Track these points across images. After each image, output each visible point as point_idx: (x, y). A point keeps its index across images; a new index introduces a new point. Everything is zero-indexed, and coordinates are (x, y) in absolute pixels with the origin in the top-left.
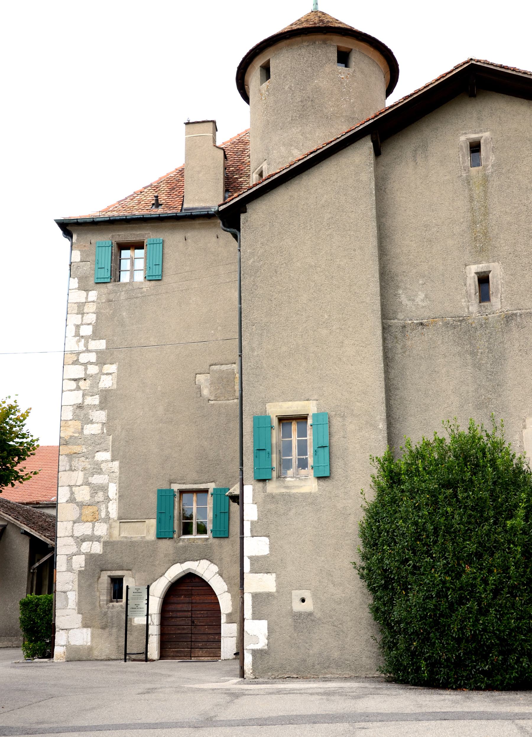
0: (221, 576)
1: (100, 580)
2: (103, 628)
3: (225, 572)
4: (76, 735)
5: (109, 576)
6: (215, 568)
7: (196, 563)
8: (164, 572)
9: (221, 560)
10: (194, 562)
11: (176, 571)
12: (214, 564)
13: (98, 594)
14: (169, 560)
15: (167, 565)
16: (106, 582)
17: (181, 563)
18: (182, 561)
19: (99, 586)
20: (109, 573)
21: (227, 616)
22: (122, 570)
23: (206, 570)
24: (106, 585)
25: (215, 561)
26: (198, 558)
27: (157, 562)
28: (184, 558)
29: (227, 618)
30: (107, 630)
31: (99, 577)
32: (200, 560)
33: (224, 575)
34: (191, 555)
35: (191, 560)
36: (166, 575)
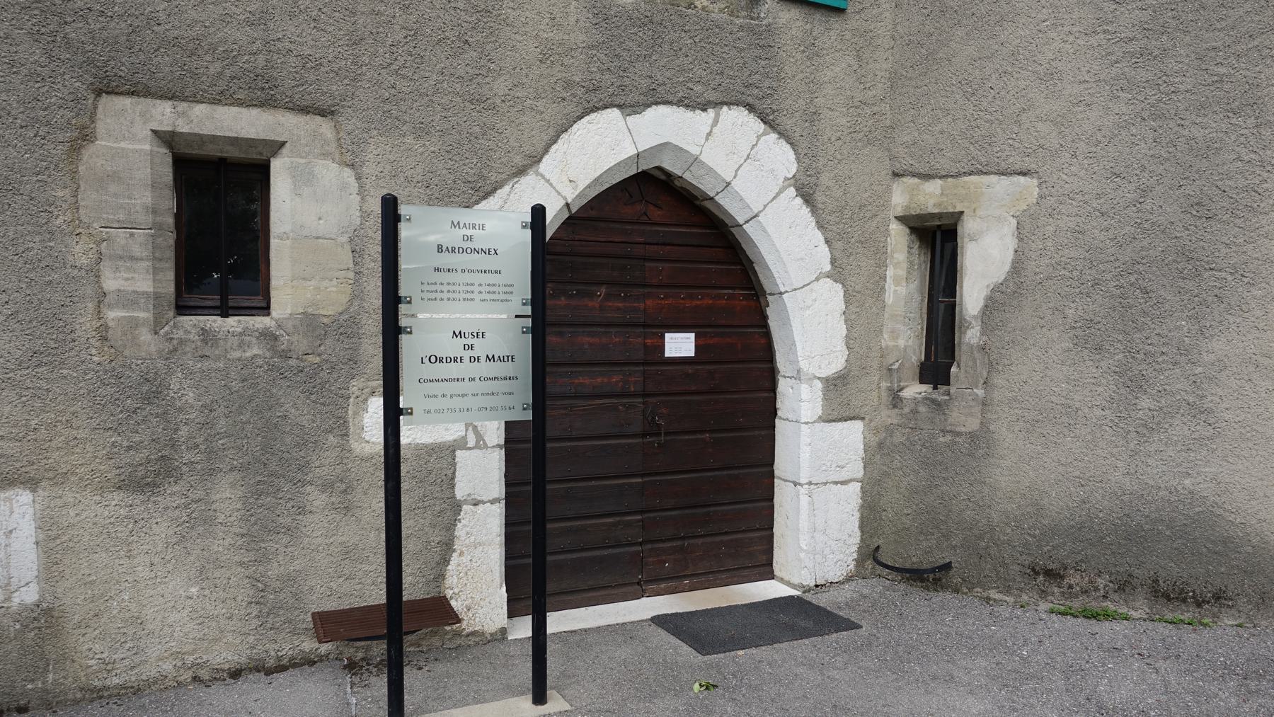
0: (808, 199)
1: (94, 158)
2: (144, 481)
3: (825, 179)
4: (1122, 684)
5: (167, 139)
6: (780, 158)
7: (703, 119)
8: (540, 146)
9: (812, 117)
10: (689, 114)
11: (588, 155)
12: (782, 135)
13: (80, 253)
14: (569, 84)
15: (571, 108)
16: (143, 172)
17: (631, 108)
18: (632, 98)
19: (89, 197)
20: (165, 115)
21: (826, 391)
22: (268, 103)
23: (740, 162)
24: (144, 198)
25: (787, 123)
26: (712, 96)
27: (501, 86)
28: (644, 83)
29: (826, 398)
30: (173, 495)
31: (85, 136)
32: (717, 104)
33: (819, 197)
34: (682, 70)
35: (679, 103)
36: (546, 165)
